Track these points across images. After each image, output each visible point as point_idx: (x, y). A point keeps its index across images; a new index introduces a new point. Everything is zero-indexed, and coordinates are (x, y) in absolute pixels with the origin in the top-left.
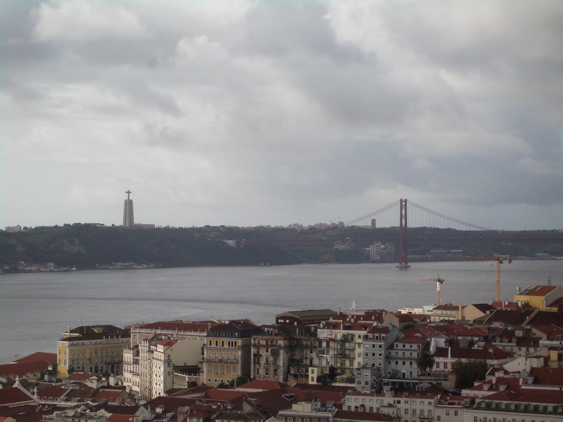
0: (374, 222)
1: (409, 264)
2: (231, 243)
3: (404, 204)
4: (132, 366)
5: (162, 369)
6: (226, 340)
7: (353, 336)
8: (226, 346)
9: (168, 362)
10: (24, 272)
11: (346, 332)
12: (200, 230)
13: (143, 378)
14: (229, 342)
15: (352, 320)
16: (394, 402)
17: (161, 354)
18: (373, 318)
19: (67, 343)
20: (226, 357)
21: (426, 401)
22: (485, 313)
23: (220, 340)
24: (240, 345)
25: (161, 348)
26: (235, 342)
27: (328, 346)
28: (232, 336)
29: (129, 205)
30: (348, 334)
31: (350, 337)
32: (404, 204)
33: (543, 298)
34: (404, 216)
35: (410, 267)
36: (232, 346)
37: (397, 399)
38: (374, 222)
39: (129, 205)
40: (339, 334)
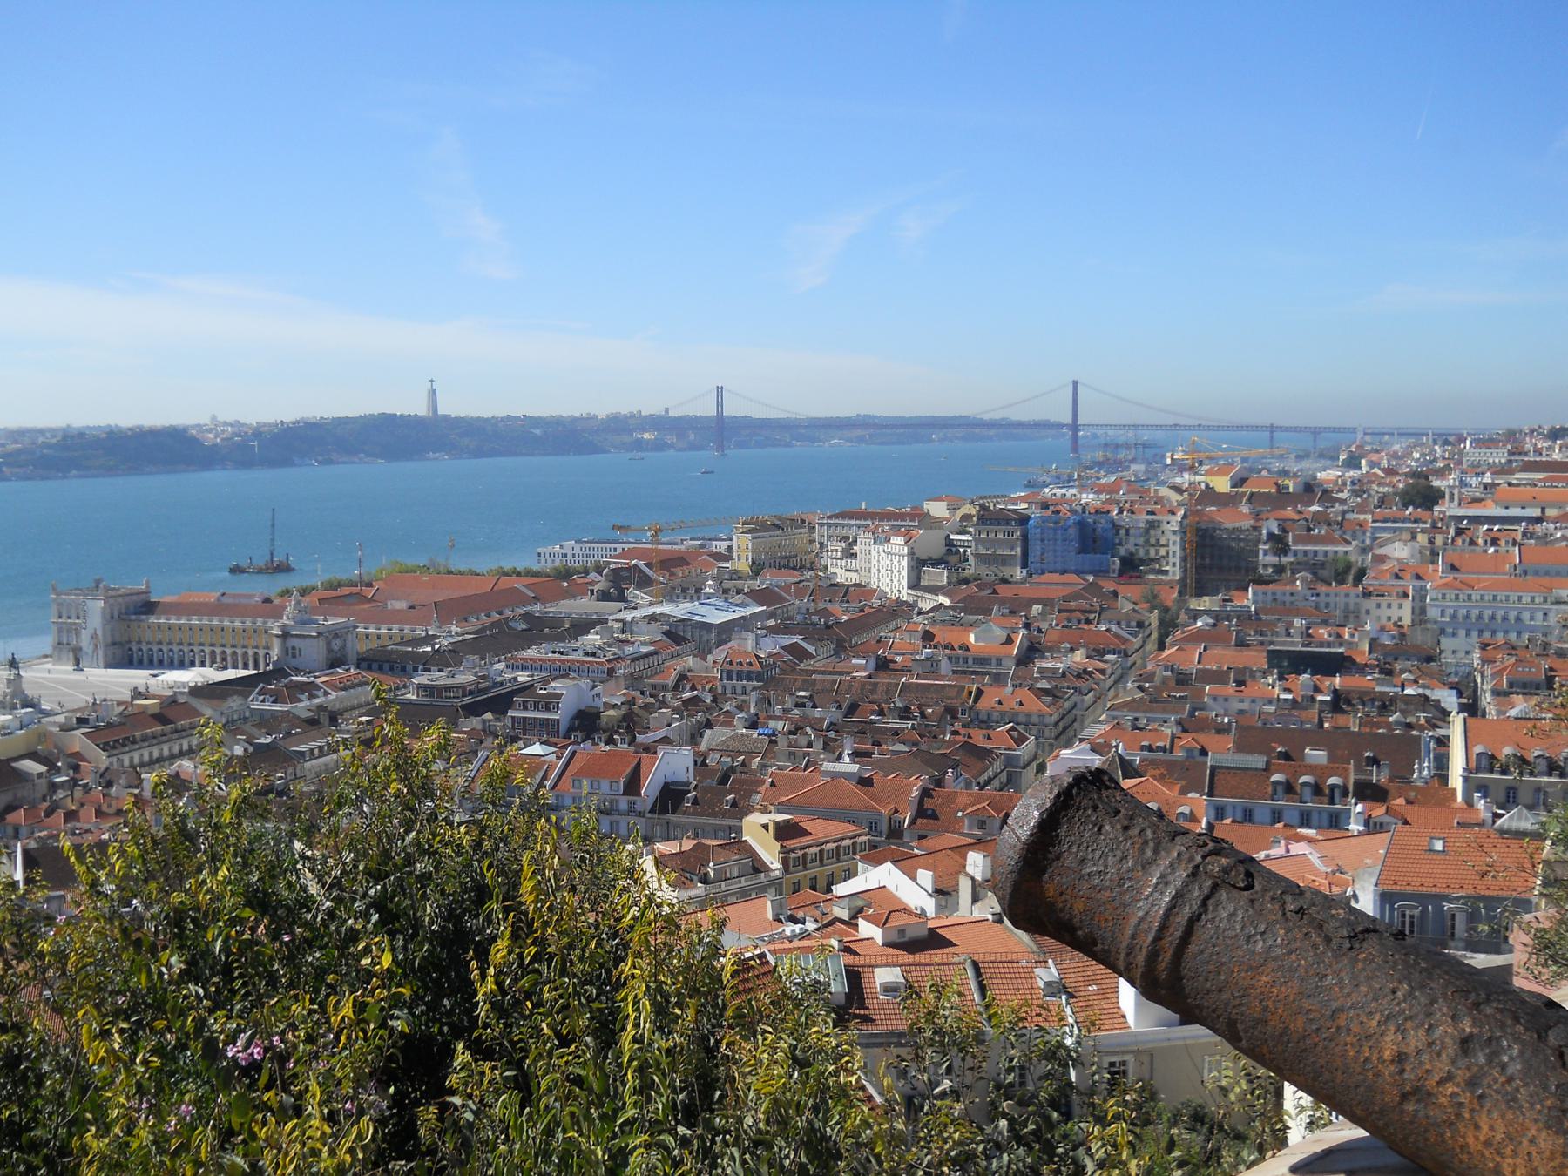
0: (667, 410)
2: (538, 432)
3: (720, 391)
5: (905, 563)
8: (1000, 536)
9: (911, 554)
10: (338, 463)
11: (1150, 517)
12: (502, 419)
13: (863, 573)
15: (1127, 505)
27: (1127, 533)
29: (433, 393)
30: (1153, 521)
32: (720, 391)
34: (720, 404)
38: (667, 410)
39: (433, 393)
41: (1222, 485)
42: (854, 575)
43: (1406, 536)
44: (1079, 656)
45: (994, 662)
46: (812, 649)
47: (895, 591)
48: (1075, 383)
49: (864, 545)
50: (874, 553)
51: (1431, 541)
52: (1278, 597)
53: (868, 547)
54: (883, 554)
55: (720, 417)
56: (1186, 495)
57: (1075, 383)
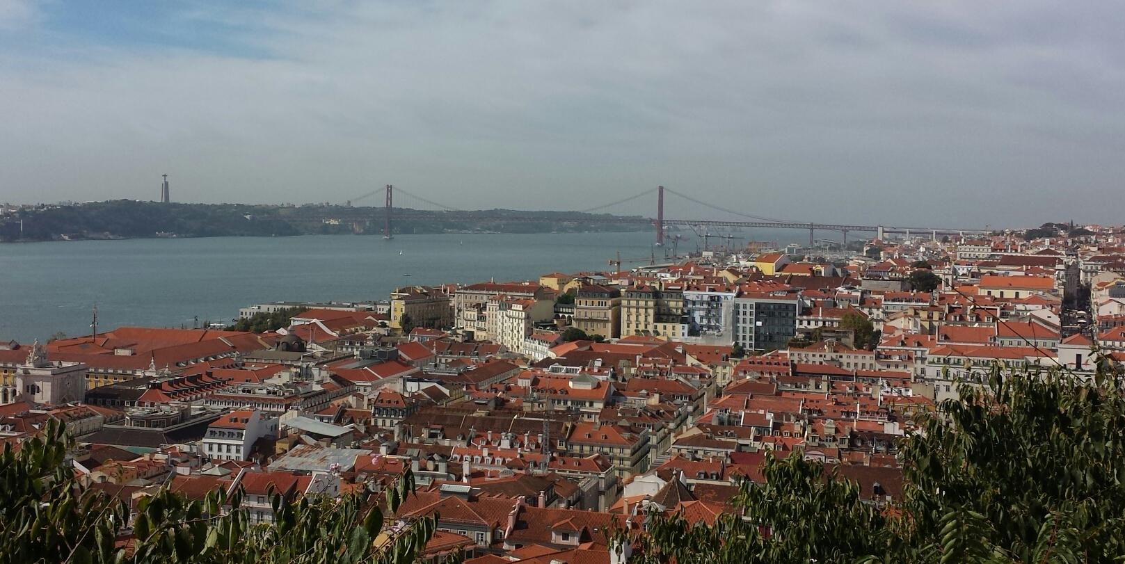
0: (349, 202)
1: (393, 236)
4: (476, 323)
5: (522, 325)
6: (596, 302)
7: (718, 297)
9: (528, 318)
13: (490, 332)
14: (599, 302)
15: (695, 284)
16: (837, 356)
17: (520, 313)
18: (714, 281)
19: (403, 302)
20: (595, 316)
21: (868, 357)
22: (738, 277)
23: (589, 302)
24: (610, 304)
25: (520, 307)
26: (605, 303)
28: (601, 296)
31: (716, 298)
33: (774, 264)
34: (389, 199)
35: (393, 238)
36: (602, 305)
37: (839, 354)
38: (349, 202)
40: (706, 295)
41: (768, 269)
42: (484, 334)
43: (911, 312)
44: (654, 400)
45: (587, 404)
46: (447, 392)
47: (515, 347)
48: (661, 189)
49: (492, 309)
50: (499, 317)
51: (930, 318)
52: (811, 359)
53: (494, 312)
54: (506, 318)
55: (389, 208)
56: (741, 276)
57: (661, 189)
